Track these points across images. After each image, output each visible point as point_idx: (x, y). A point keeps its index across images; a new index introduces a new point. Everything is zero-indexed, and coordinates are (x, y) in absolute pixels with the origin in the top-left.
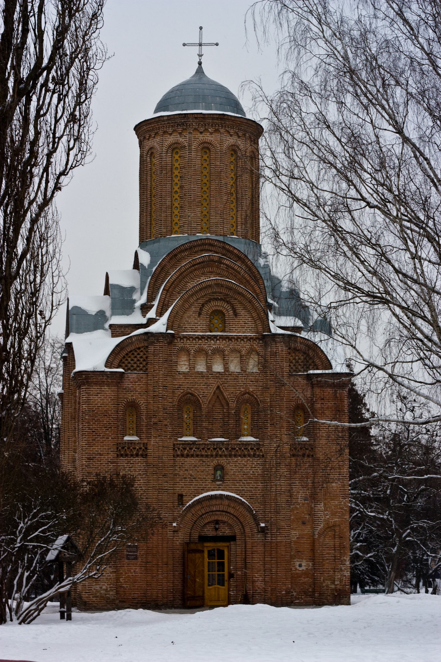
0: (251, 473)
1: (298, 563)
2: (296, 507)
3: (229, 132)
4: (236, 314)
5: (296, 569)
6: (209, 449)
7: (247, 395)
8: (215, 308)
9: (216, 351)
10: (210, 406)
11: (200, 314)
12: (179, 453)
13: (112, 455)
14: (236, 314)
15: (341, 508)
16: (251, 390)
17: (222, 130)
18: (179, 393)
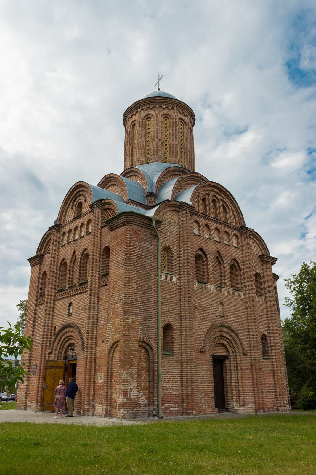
0: (83, 305)
1: (99, 376)
2: (100, 328)
3: (143, 109)
4: (85, 201)
5: (98, 381)
6: (68, 292)
7: (86, 251)
8: (79, 201)
9: (76, 228)
10: (72, 263)
11: (72, 208)
12: (57, 298)
13: (34, 305)
14: (85, 201)
15: (121, 325)
16: (87, 246)
17: (139, 110)
18: (60, 260)
